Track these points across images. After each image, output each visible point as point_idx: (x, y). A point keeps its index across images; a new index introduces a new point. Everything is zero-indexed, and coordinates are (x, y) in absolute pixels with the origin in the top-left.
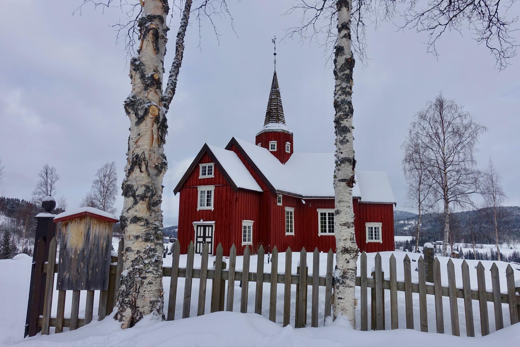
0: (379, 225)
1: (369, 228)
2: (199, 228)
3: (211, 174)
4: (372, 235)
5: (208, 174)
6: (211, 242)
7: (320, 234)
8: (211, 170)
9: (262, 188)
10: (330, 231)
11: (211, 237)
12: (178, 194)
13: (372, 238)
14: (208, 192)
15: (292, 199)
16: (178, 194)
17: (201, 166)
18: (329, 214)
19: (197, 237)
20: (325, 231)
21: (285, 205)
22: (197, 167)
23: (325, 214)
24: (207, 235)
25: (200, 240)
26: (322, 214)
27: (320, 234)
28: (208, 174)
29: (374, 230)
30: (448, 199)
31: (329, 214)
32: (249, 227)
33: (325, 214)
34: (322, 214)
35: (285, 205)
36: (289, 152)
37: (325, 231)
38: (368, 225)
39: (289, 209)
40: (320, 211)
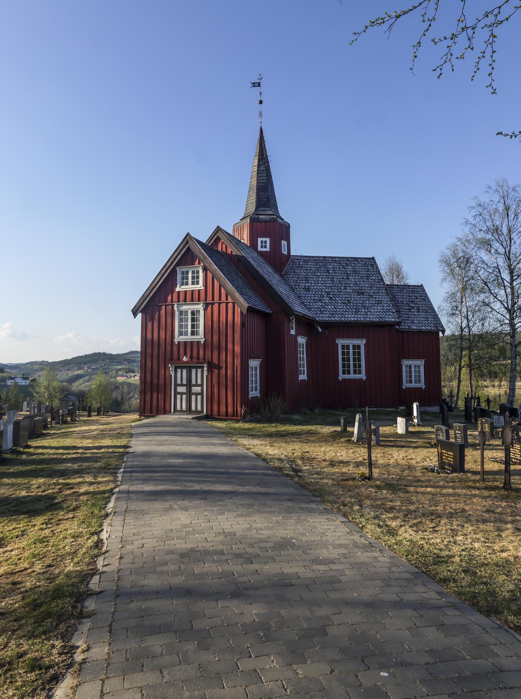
0: (421, 363)
1: (406, 366)
2: (179, 370)
3: (198, 283)
4: (411, 377)
5: (193, 283)
6: (202, 394)
7: (341, 376)
8: (198, 277)
9: (269, 307)
10: (355, 373)
11: (202, 385)
12: (140, 315)
13: (411, 382)
14: (193, 313)
15: (307, 325)
16: (140, 315)
17: (179, 270)
18: (354, 347)
19: (176, 385)
20: (349, 373)
21: (297, 334)
22: (174, 271)
23: (348, 347)
24: (194, 382)
25: (180, 389)
26: (343, 347)
27: (341, 376)
28: (193, 283)
29: (413, 370)
30: (515, 325)
31: (354, 347)
32: (256, 368)
33: (348, 347)
34: (343, 347)
35: (297, 334)
36: (285, 253)
37: (349, 373)
38: (405, 363)
39: (301, 340)
40: (341, 342)
